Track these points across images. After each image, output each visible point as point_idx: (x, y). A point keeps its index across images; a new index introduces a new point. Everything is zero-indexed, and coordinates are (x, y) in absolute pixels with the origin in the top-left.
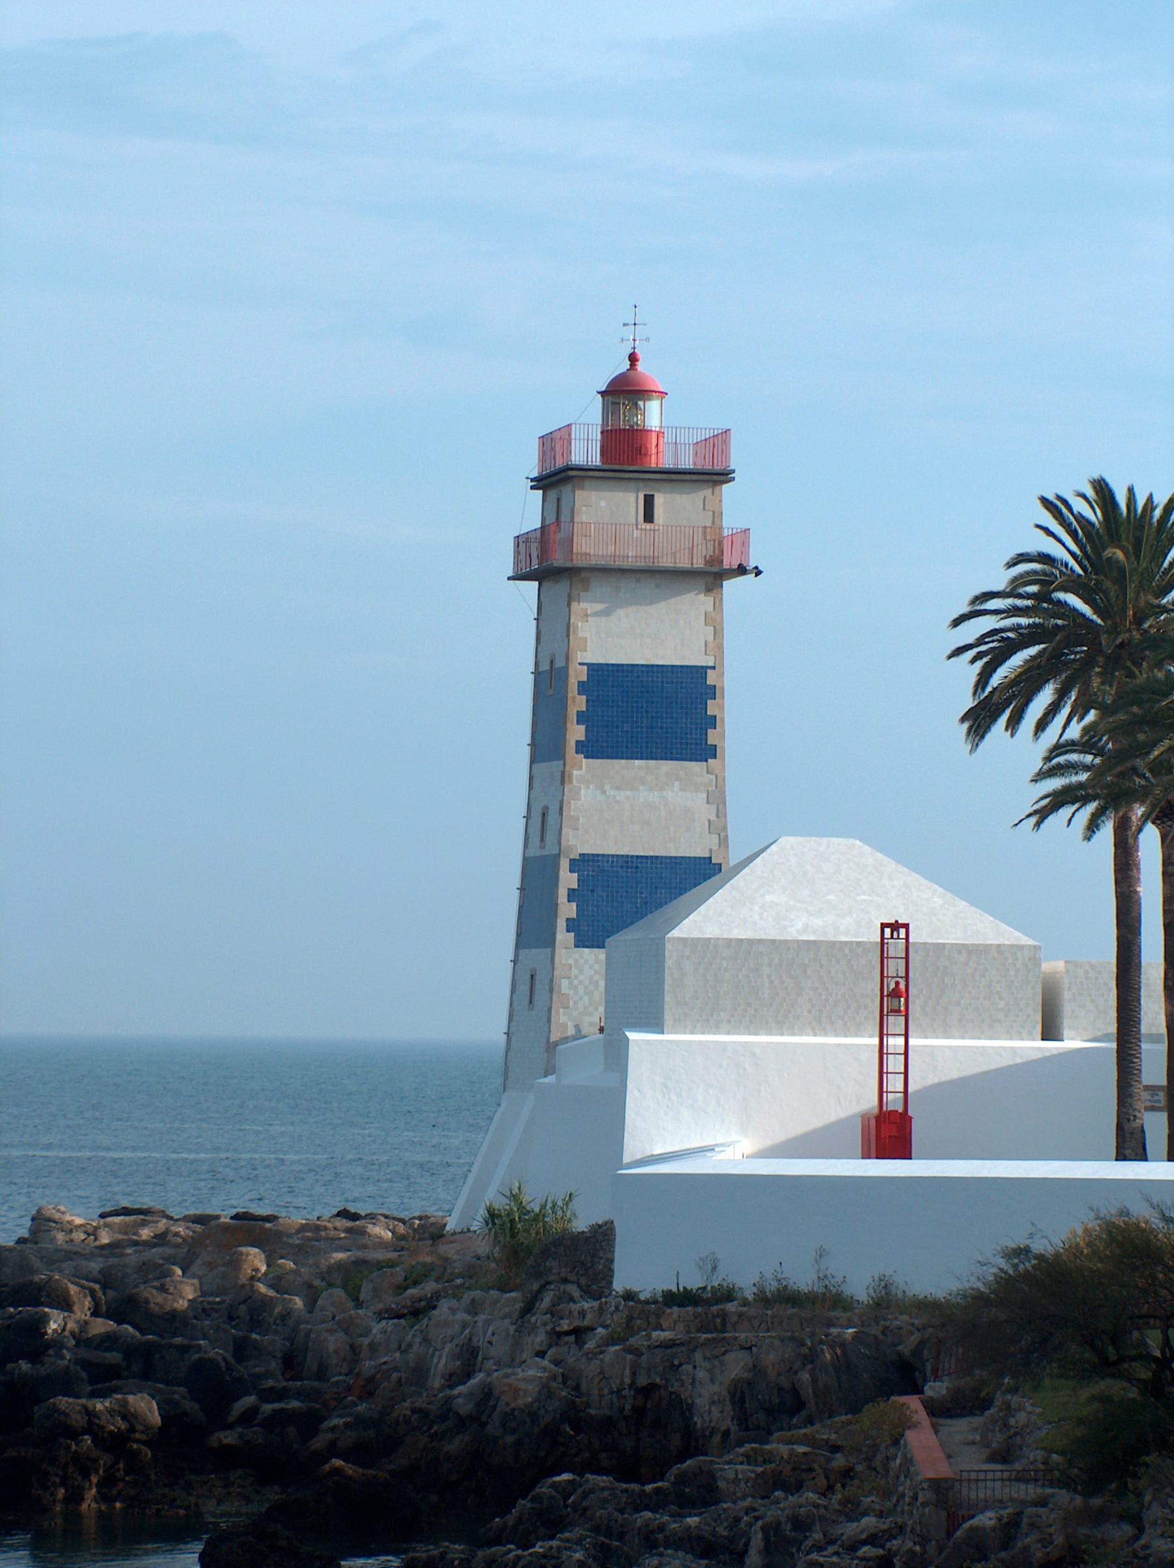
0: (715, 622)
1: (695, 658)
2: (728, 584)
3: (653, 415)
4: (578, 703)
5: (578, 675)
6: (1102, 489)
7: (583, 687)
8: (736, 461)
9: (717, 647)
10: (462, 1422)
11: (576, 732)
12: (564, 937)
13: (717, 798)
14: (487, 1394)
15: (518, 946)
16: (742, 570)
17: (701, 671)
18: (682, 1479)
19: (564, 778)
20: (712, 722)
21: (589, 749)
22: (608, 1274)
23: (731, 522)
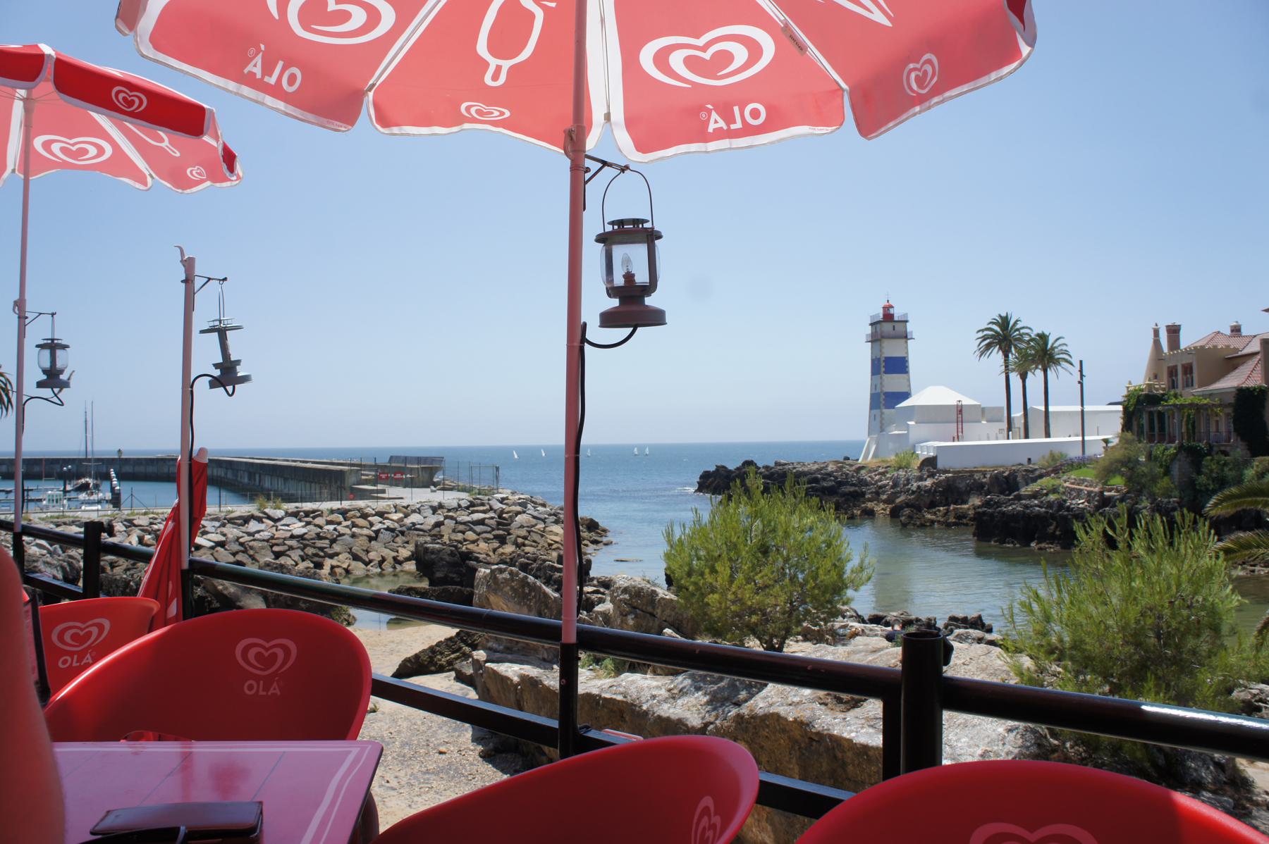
0: (907, 348)
1: (905, 355)
2: (909, 341)
3: (891, 311)
4: (883, 364)
5: (883, 359)
6: (1000, 316)
7: (884, 361)
8: (909, 319)
9: (907, 353)
10: (913, 492)
11: (883, 369)
12: (882, 407)
13: (909, 380)
14: (919, 487)
15: (871, 408)
16: (912, 339)
17: (905, 358)
18: (1015, 496)
19: (881, 378)
20: (907, 367)
21: (886, 372)
22: (936, 465)
23: (908, 330)
